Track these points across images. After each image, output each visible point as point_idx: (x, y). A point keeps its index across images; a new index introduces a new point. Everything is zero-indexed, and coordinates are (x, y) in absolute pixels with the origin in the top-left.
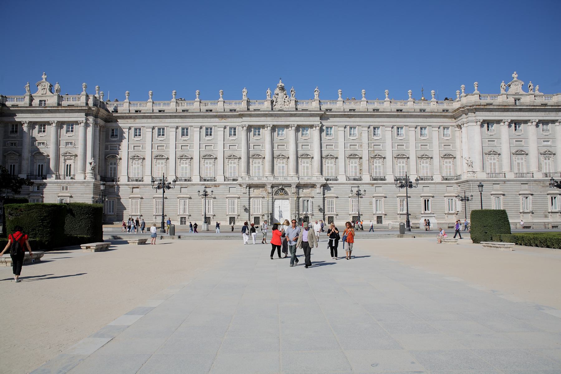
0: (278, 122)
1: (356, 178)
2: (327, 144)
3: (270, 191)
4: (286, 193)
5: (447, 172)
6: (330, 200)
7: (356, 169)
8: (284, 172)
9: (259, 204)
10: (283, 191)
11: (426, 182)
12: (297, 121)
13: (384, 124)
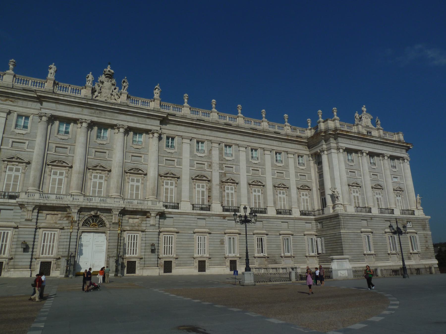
0: (100, 119)
1: (203, 206)
2: (167, 158)
3: (76, 218)
4: (101, 224)
5: (304, 205)
6: (168, 236)
7: (203, 195)
8: (102, 191)
9: (54, 239)
10: (96, 220)
11: (285, 216)
12: (128, 122)
13: (238, 142)
